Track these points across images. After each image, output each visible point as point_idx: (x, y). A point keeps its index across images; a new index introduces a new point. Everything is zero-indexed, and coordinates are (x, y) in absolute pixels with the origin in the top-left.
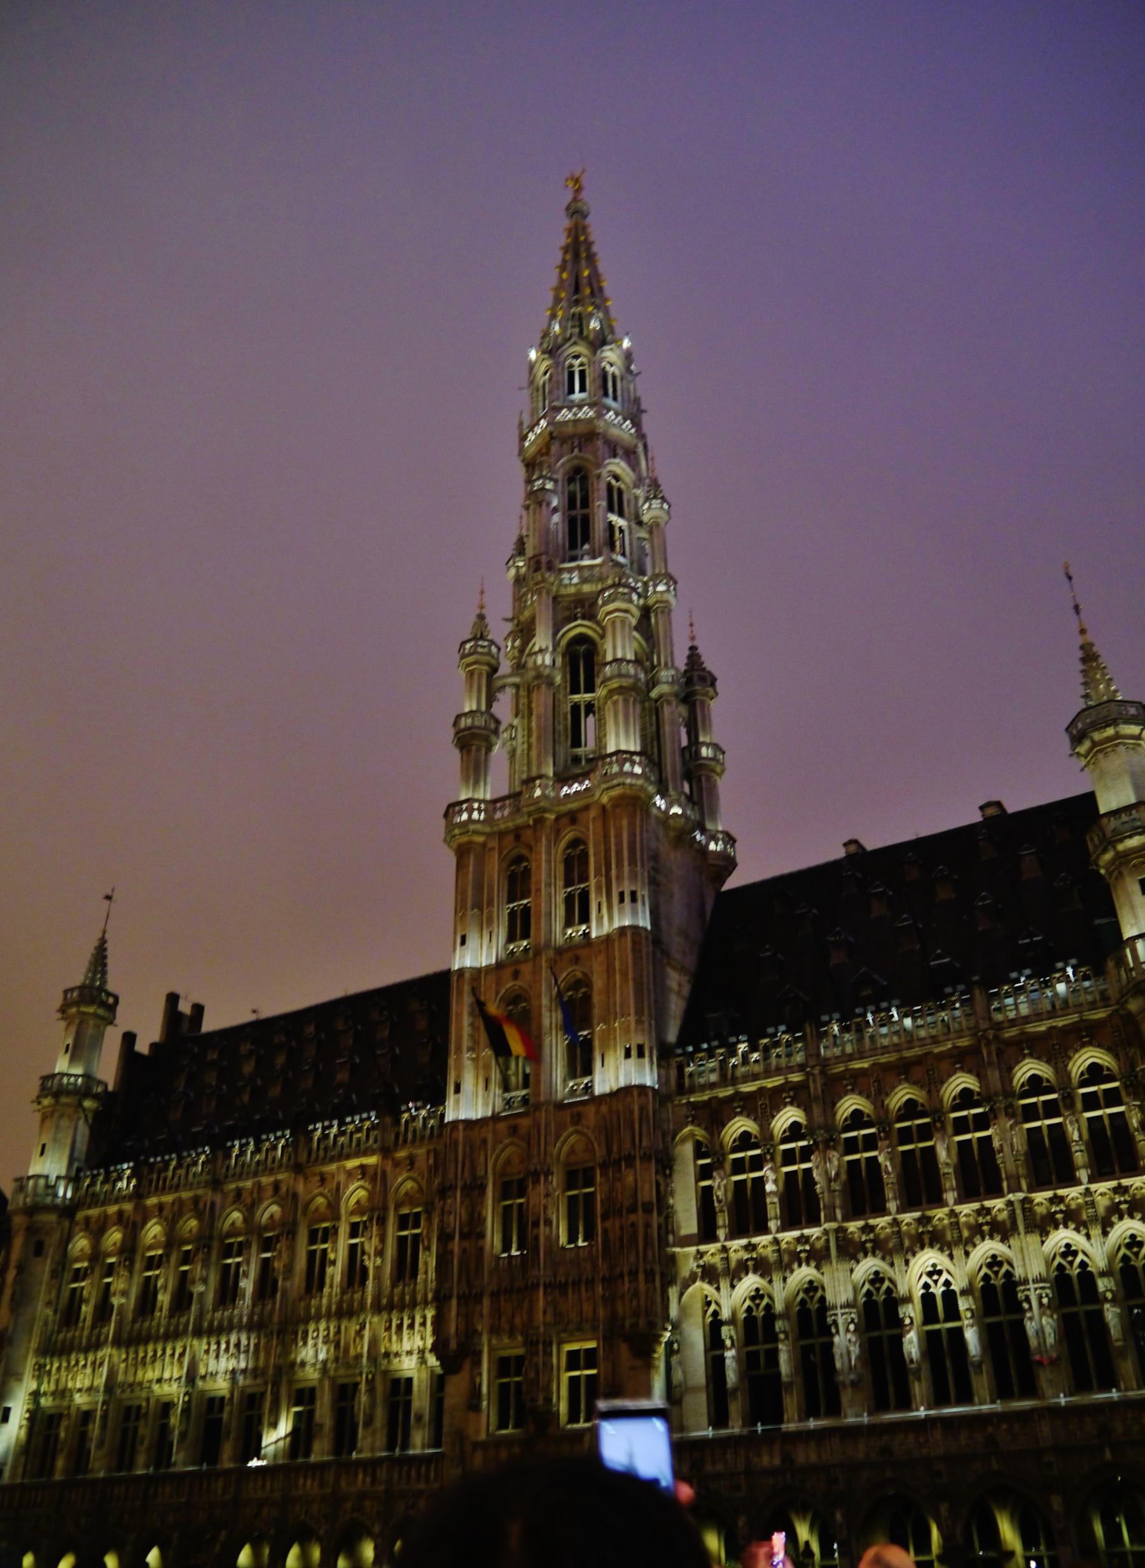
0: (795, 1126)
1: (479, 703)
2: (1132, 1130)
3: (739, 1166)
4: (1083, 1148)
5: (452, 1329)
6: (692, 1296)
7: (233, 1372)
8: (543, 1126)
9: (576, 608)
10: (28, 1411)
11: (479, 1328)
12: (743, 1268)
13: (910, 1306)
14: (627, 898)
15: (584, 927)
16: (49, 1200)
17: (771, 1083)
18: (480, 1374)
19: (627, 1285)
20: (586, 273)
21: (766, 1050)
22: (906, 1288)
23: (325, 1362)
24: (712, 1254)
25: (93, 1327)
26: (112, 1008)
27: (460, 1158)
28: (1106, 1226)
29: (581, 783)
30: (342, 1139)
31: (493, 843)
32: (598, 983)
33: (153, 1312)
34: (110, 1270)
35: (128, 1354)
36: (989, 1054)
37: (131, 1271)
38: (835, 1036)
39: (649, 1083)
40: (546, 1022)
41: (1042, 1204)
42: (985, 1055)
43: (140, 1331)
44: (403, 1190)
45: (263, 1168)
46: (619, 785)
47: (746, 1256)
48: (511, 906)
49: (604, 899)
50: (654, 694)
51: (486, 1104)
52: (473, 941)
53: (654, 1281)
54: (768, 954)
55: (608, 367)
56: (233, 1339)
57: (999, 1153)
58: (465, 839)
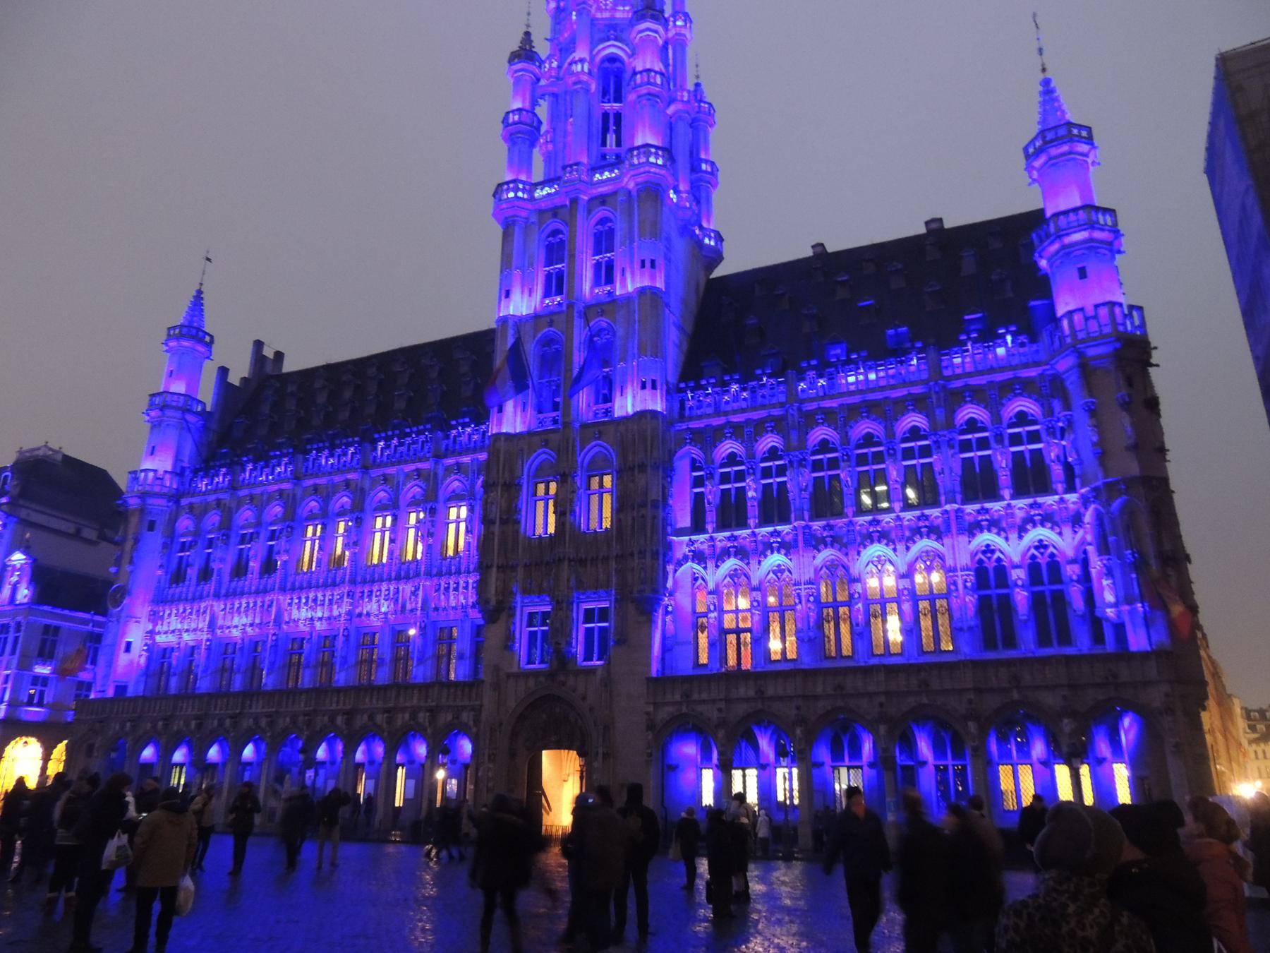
0: (774, 449)
1: (524, 102)
2: (1047, 461)
3: (725, 478)
4: (1009, 473)
5: (492, 590)
6: (682, 573)
7: (312, 619)
10: (146, 645)
11: (514, 590)
12: (725, 554)
13: (859, 584)
14: (648, 264)
16: (157, 489)
17: (755, 415)
18: (514, 624)
19: (637, 561)
21: (753, 392)
22: (857, 572)
23: (385, 614)
24: (701, 543)
25: (198, 585)
26: (209, 345)
28: (1022, 531)
29: (611, 171)
30: (401, 448)
31: (534, 218)
32: (620, 332)
33: (246, 574)
34: (210, 543)
35: (226, 605)
36: (938, 399)
37: (227, 544)
39: (659, 409)
41: (971, 514)
42: (934, 401)
43: (235, 590)
44: (450, 489)
45: (339, 469)
47: (729, 545)
52: (516, 295)
53: (658, 559)
56: (311, 595)
57: (940, 474)
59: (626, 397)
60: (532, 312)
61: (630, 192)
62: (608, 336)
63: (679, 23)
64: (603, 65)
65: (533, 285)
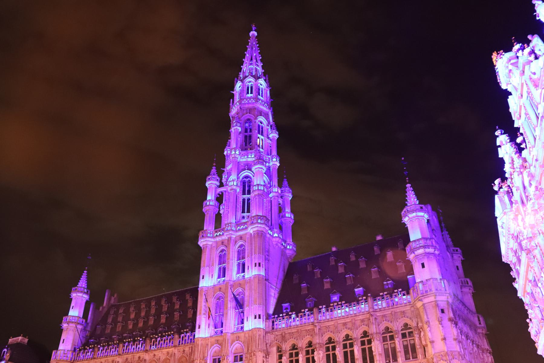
8: (227, 340)
9: (245, 166)
14: (257, 265)
15: (243, 274)
20: (255, 55)
27: (199, 350)
38: (324, 313)
40: (229, 306)
46: (256, 227)
48: (219, 266)
49: (250, 266)
50: (271, 195)
51: (208, 333)
54: (304, 284)
55: (260, 86)
58: (205, 243)
59: (249, 322)
60: (213, 285)
61: (251, 234)
62: (242, 295)
63: (274, 160)
64: (243, 180)
65: (213, 273)
